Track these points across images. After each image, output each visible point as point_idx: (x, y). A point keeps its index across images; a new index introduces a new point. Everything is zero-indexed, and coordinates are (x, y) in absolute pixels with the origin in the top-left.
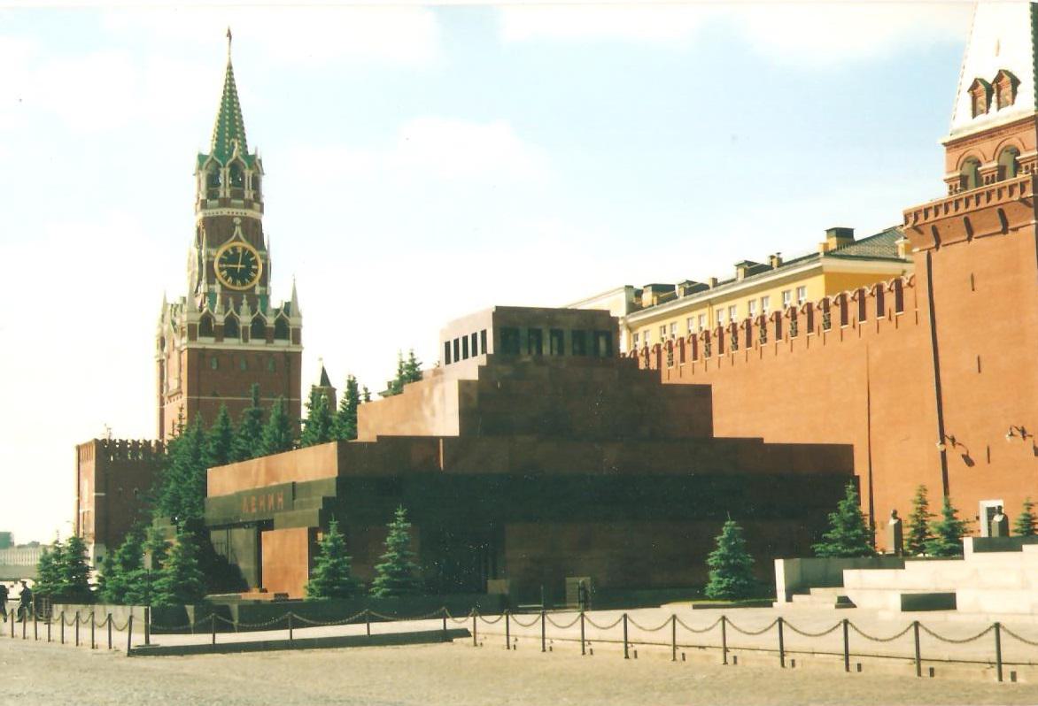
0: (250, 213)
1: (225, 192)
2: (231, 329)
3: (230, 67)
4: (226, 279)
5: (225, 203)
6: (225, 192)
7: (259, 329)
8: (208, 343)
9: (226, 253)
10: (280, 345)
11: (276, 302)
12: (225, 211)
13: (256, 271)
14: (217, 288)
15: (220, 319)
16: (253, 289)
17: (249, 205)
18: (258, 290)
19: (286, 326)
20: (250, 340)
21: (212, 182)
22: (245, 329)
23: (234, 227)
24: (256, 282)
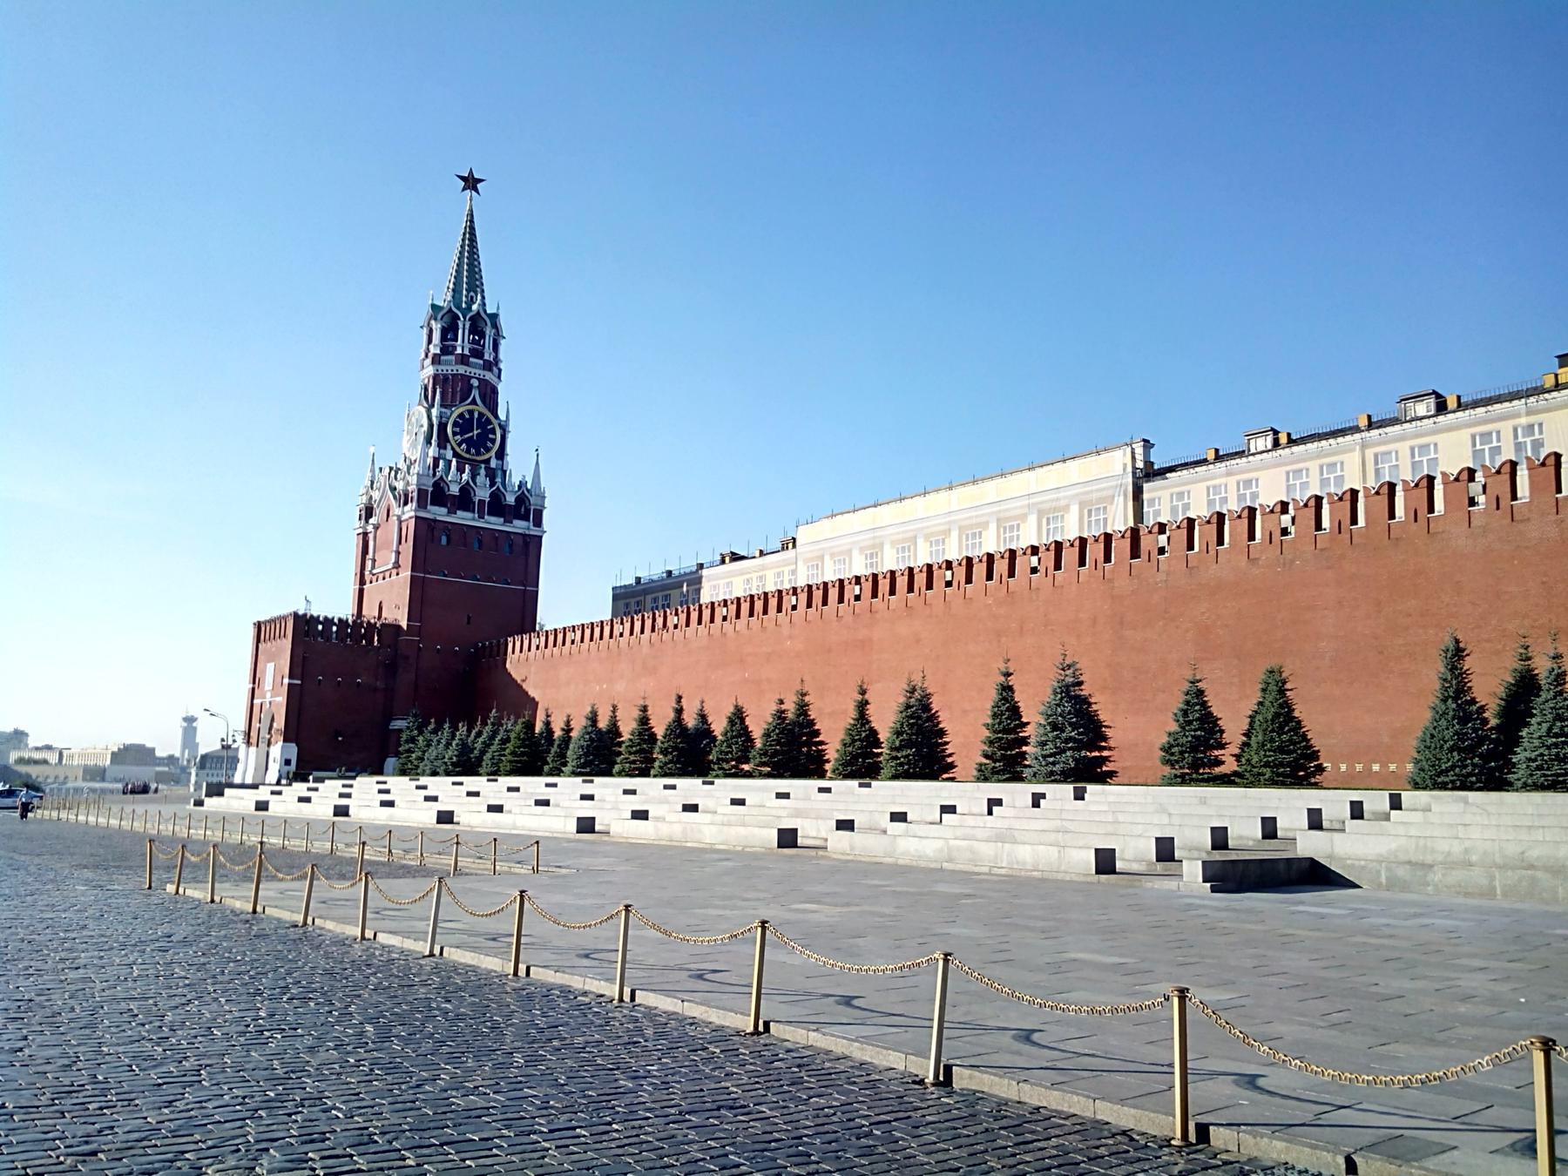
0: (489, 376)
1: (462, 345)
2: (464, 500)
4: (459, 445)
5: (463, 360)
6: (462, 345)
7: (496, 505)
8: (439, 513)
9: (461, 416)
10: (519, 526)
11: (516, 481)
12: (462, 369)
13: (493, 441)
14: (449, 454)
15: (454, 489)
16: (487, 461)
17: (488, 366)
18: (493, 463)
19: (526, 507)
21: (449, 332)
22: (481, 502)
24: (493, 453)
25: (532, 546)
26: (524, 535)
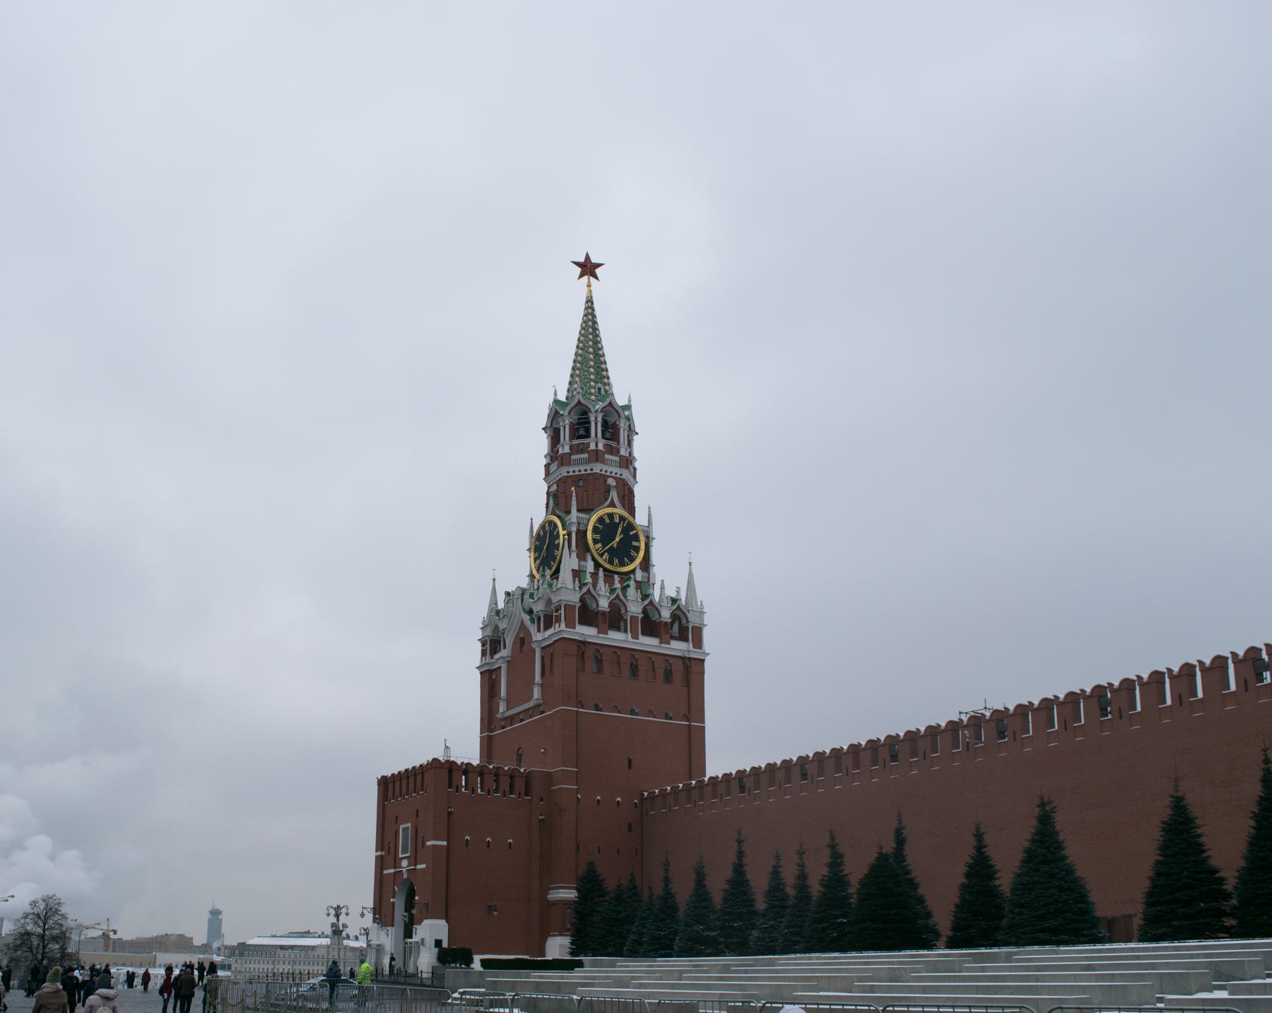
0: (626, 475)
1: (596, 441)
2: (615, 619)
3: (590, 301)
5: (596, 456)
8: (587, 632)
9: (601, 520)
10: (677, 647)
12: (598, 468)
13: (637, 549)
14: (590, 567)
15: (604, 604)
20: (641, 637)
21: (581, 428)
22: (633, 618)
23: (609, 491)
25: (689, 674)
26: (683, 658)
